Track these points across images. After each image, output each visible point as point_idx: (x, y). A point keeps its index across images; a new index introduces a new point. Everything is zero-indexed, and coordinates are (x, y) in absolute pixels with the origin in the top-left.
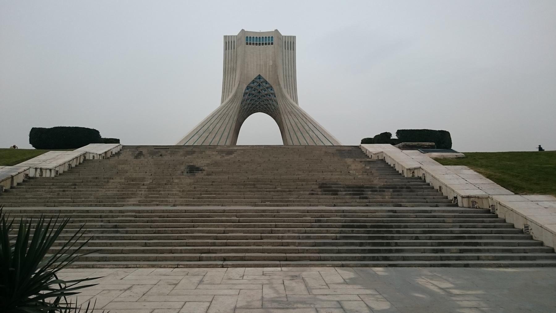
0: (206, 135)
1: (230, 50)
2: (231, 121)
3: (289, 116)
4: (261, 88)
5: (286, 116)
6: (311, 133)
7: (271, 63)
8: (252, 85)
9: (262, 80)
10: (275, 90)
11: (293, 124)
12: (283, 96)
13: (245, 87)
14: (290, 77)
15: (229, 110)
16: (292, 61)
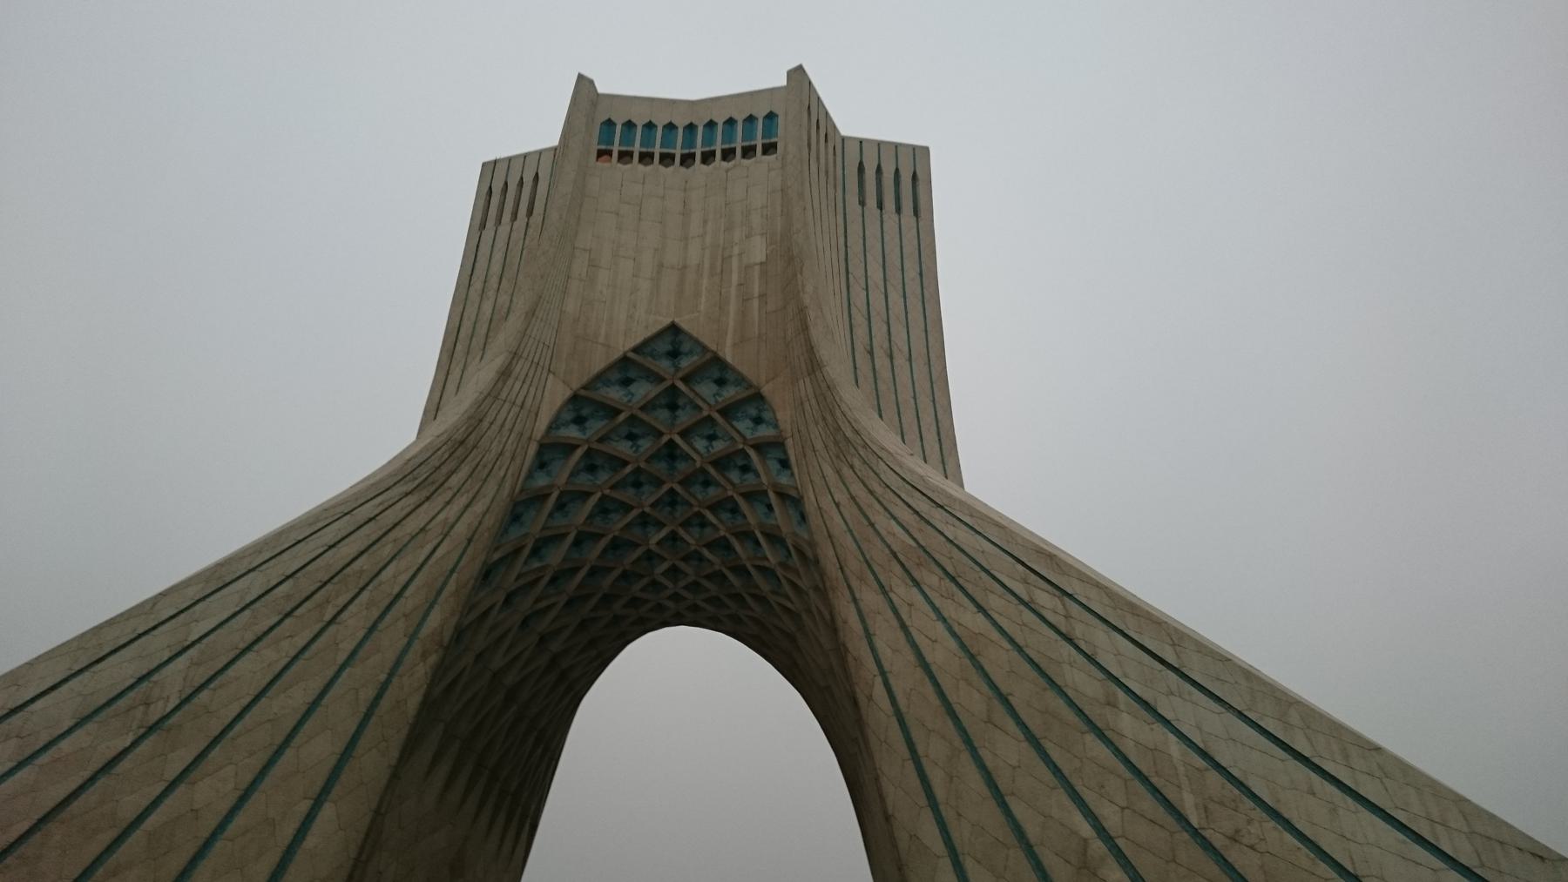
0: (103, 741)
1: (504, 229)
2: (391, 639)
3: (902, 592)
4: (685, 418)
5: (870, 598)
6: (1129, 726)
7: (758, 250)
8: (615, 394)
9: (685, 363)
10: (785, 416)
11: (942, 653)
12: (847, 445)
13: (555, 395)
14: (900, 361)
15: (386, 550)
16: (912, 273)
